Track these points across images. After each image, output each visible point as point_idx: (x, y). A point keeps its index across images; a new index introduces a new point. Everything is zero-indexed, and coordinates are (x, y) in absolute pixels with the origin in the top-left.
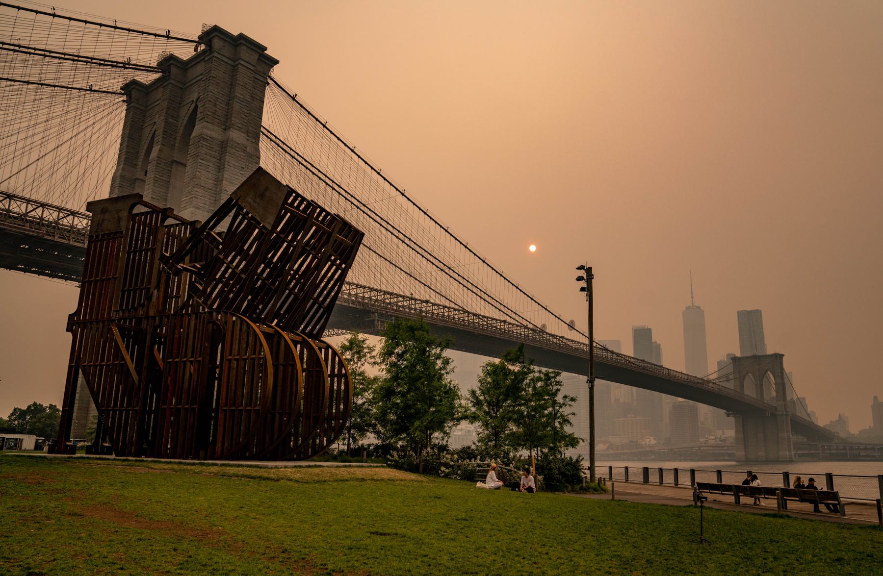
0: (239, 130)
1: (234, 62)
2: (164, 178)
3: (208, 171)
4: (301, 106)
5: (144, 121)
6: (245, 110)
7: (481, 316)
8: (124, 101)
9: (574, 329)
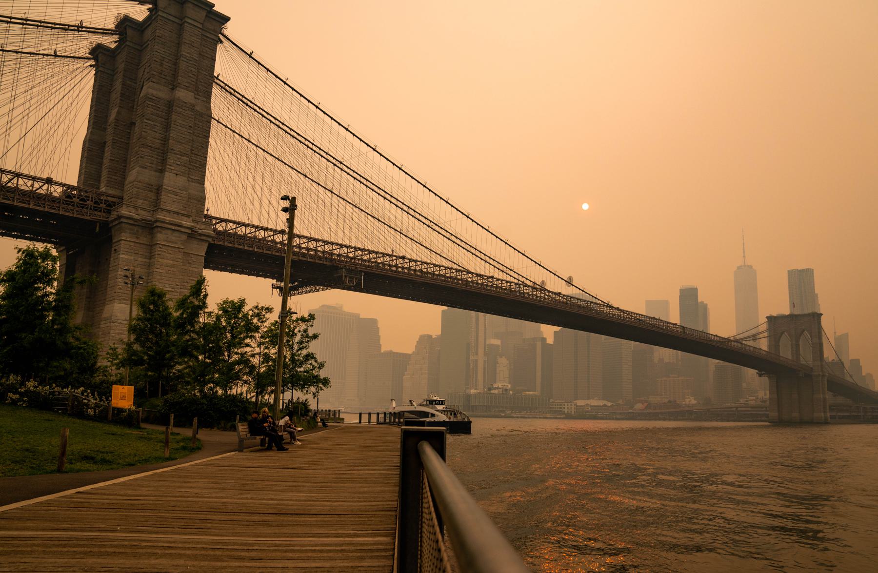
0: (186, 90)
1: (182, 20)
2: (123, 140)
3: (154, 131)
4: (259, 63)
5: (112, 85)
6: (193, 69)
7: (485, 276)
8: (91, 66)
9: (573, 285)
